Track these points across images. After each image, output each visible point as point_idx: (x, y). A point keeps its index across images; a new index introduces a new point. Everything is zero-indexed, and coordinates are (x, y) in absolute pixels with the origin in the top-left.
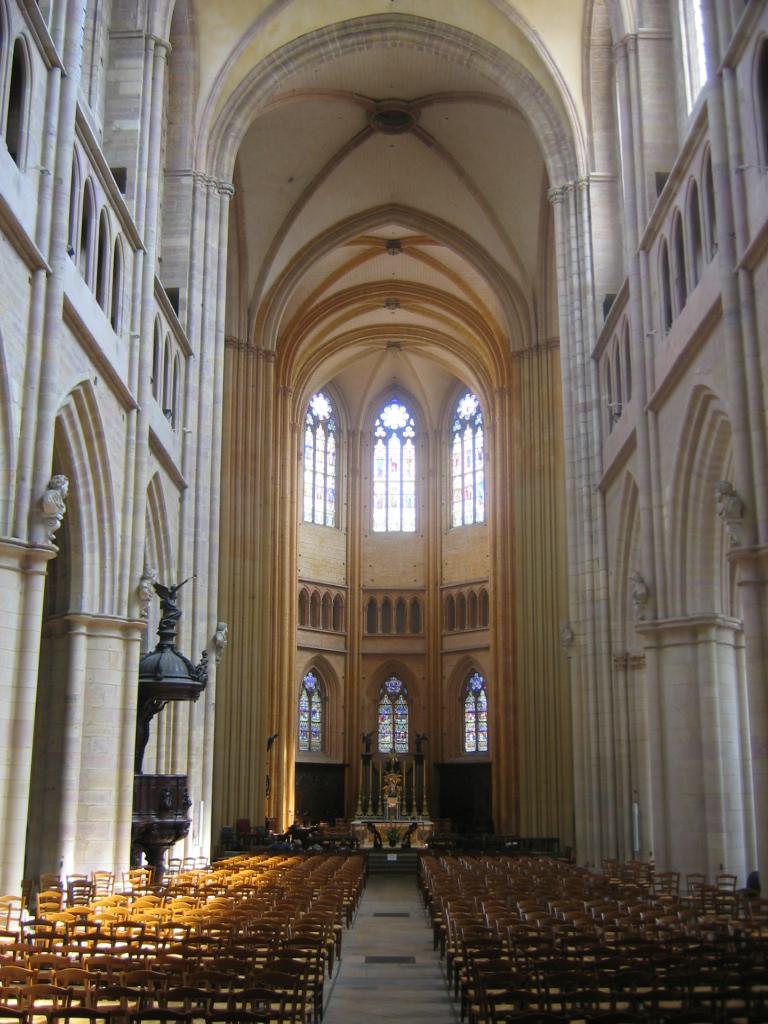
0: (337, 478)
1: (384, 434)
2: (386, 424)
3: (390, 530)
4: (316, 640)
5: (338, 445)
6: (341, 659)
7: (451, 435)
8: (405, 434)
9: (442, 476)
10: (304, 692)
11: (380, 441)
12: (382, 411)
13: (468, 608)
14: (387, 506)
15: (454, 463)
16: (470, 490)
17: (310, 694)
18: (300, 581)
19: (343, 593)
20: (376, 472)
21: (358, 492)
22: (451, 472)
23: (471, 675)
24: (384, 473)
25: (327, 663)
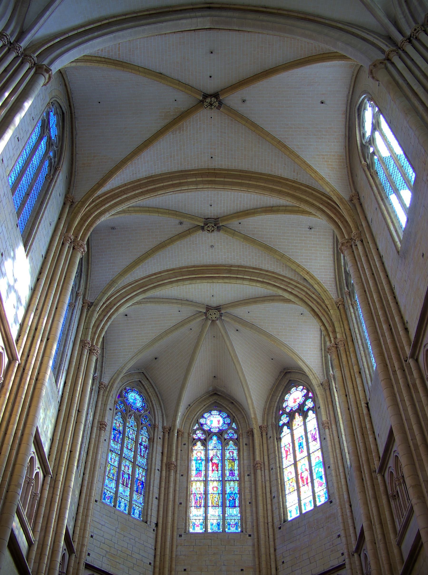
0: (148, 471)
3: (210, 451)
5: (151, 440)
7: (279, 430)
8: (226, 436)
9: (270, 469)
11: (199, 444)
14: (206, 506)
15: (284, 455)
16: (306, 474)
20: (194, 473)
21: (172, 485)
22: (281, 462)
24: (203, 473)
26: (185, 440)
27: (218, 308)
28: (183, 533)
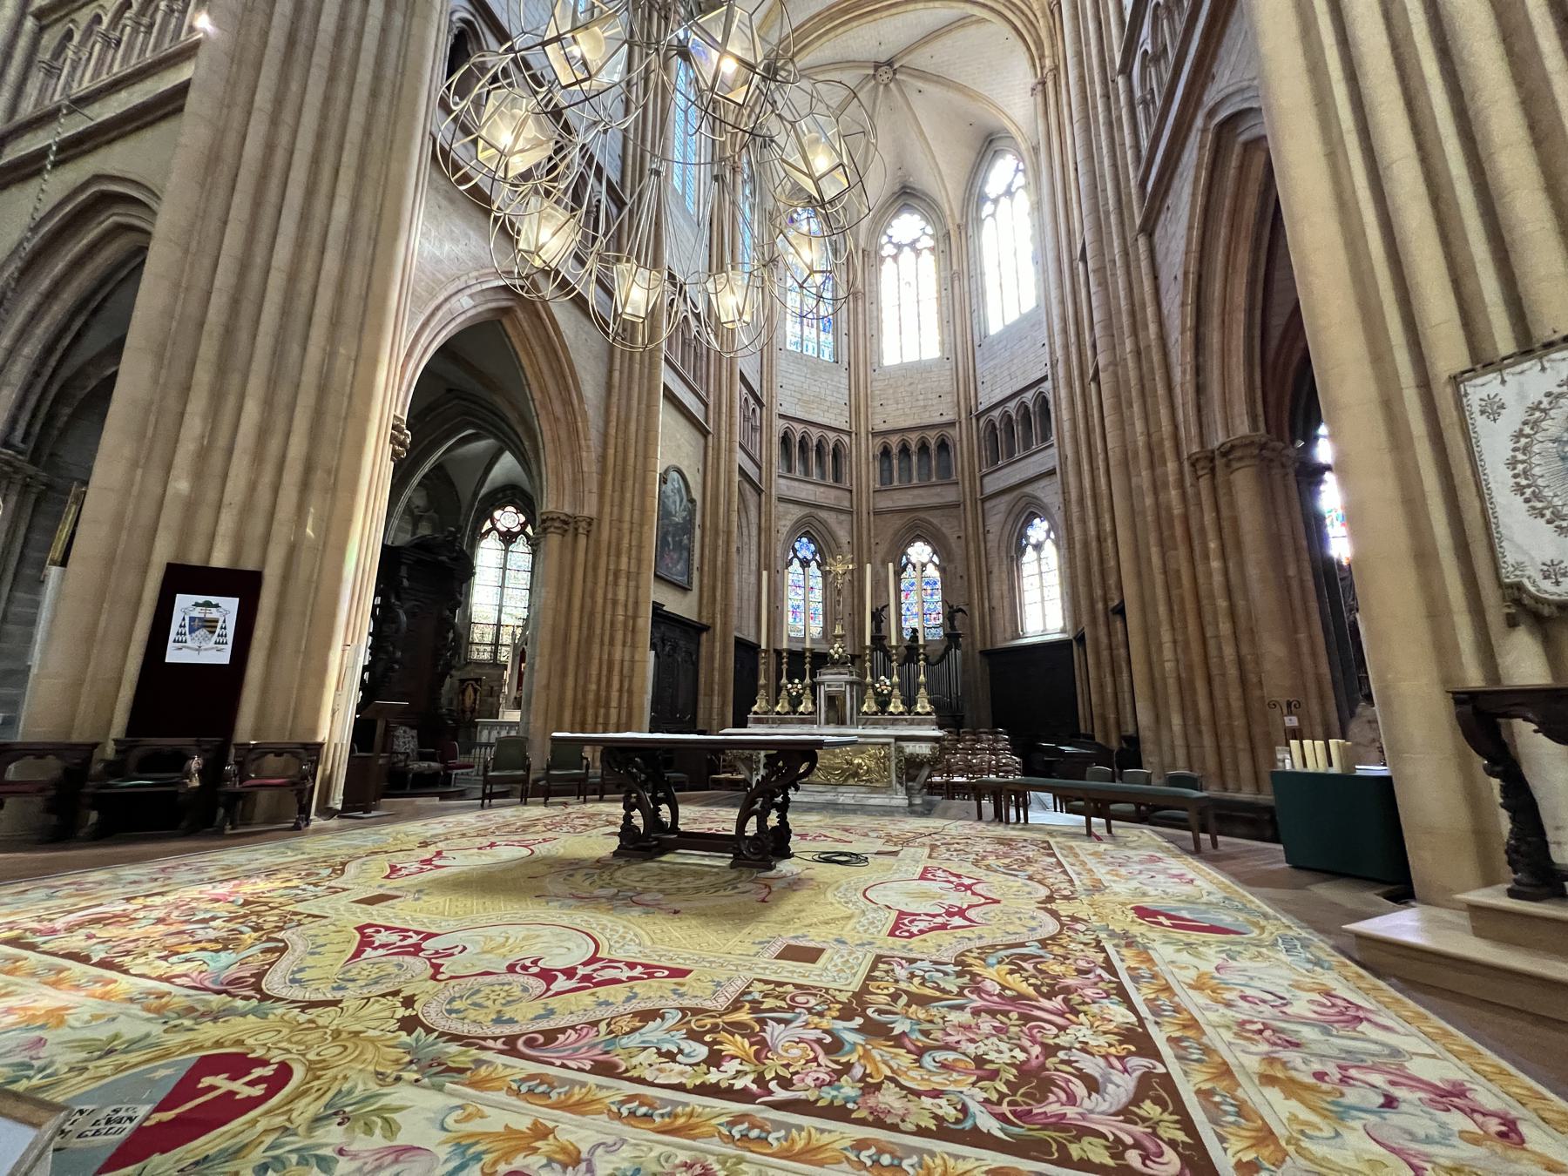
1: (893, 251)
2: (894, 240)
4: (805, 492)
6: (843, 517)
10: (796, 562)
11: (889, 260)
12: (889, 225)
13: (1018, 430)
17: (805, 563)
18: (782, 416)
19: (846, 439)
21: (860, 316)
23: (1028, 522)
25: (823, 522)
26: (872, 260)
27: (890, 63)
28: (876, 367)
